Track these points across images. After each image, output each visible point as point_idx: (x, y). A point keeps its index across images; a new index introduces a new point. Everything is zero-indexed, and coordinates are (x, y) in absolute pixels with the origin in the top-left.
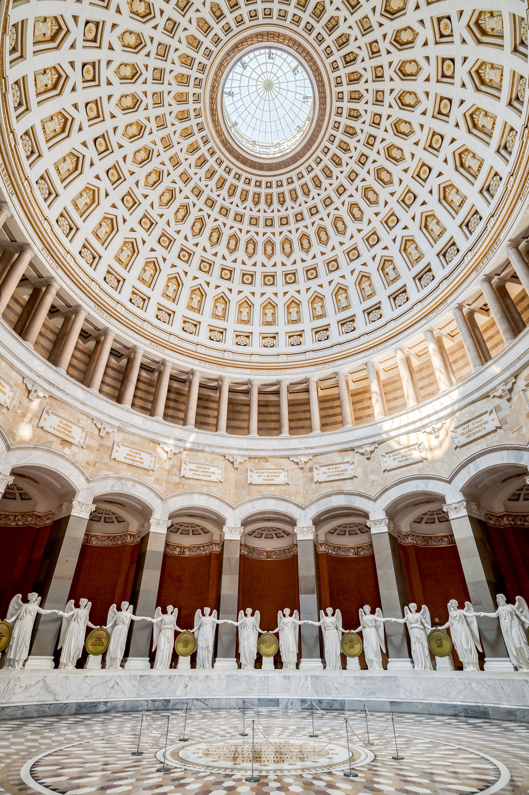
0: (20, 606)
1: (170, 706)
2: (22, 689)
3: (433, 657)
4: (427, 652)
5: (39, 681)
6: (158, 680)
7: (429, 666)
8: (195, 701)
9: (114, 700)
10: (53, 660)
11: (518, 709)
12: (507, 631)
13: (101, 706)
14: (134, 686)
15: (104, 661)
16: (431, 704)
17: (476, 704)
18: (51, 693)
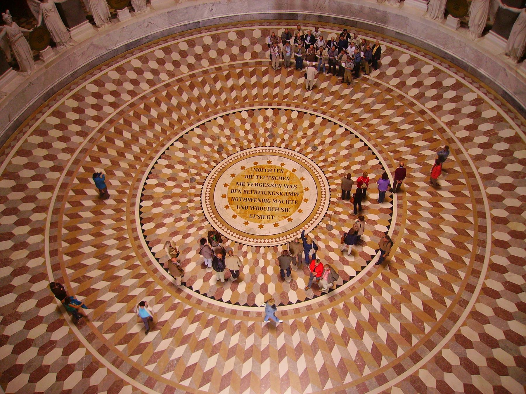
0: (39, 4)
1: (201, 25)
2: (81, 56)
3: (446, 15)
4: (443, 7)
5: (89, 47)
6: (185, 11)
7: (440, 16)
8: (222, 18)
9: (152, 33)
10: (89, 22)
11: (488, 78)
12: (515, 33)
13: (144, 40)
14: (165, 20)
15: (132, 10)
16: (428, 45)
17: (462, 60)
18: (102, 48)
